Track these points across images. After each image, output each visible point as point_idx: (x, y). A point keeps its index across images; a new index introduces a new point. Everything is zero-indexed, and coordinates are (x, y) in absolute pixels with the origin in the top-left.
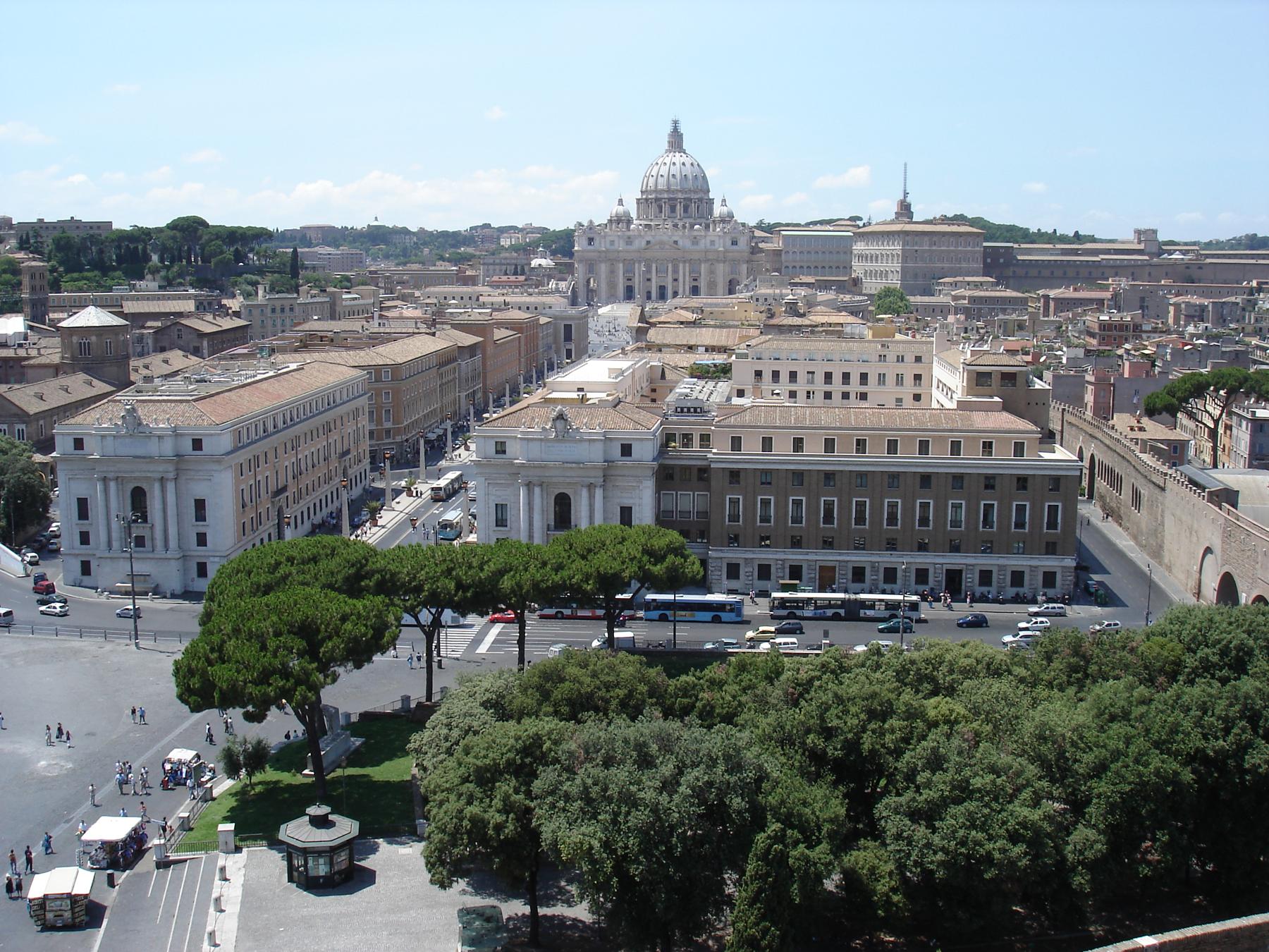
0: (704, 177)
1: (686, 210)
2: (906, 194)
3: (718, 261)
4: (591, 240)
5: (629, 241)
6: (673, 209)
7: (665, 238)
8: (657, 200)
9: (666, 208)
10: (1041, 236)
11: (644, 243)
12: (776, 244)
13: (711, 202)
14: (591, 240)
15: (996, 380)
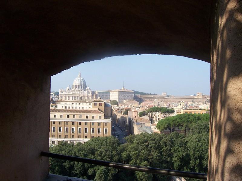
0: (85, 82)
1: (81, 87)
2: (124, 86)
3: (86, 97)
4: (62, 92)
5: (69, 92)
6: (79, 87)
7: (76, 92)
8: (76, 86)
9: (77, 87)
10: (148, 94)
11: (72, 93)
12: (97, 93)
13: (86, 87)
14: (62, 92)
15: (98, 104)
